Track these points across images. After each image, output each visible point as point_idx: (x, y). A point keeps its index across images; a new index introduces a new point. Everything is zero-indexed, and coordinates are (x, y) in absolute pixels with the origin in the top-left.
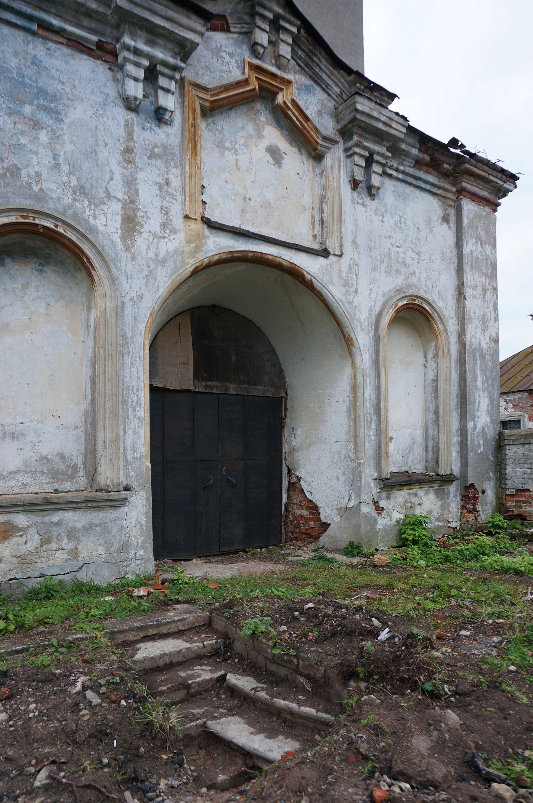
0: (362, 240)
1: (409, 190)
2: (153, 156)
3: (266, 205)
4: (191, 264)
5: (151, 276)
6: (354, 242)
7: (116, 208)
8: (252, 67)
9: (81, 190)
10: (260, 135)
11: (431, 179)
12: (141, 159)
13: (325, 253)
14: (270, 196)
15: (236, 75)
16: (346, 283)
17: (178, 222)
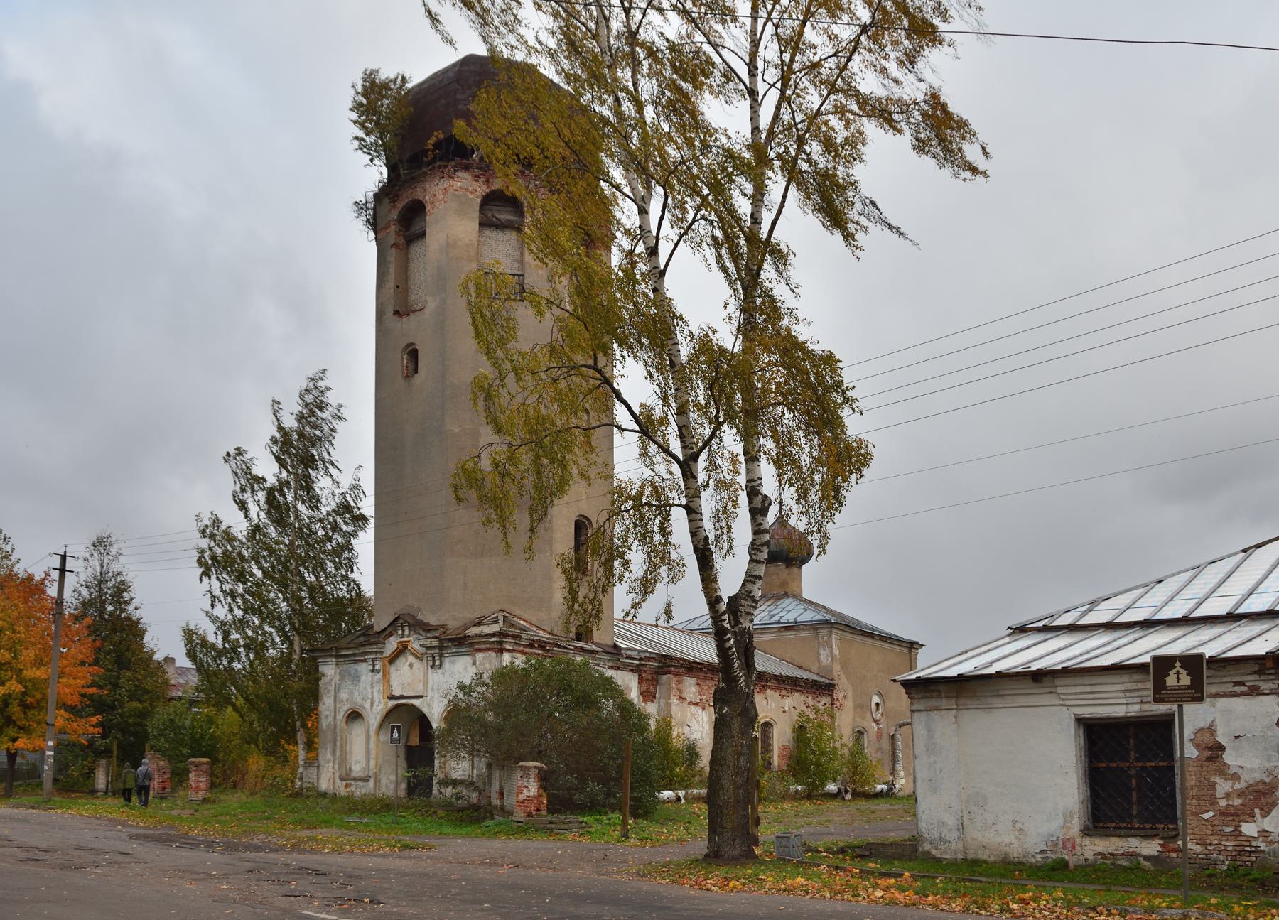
0: (435, 687)
1: (456, 658)
2: (377, 683)
3: (409, 684)
4: (385, 711)
5: (376, 718)
6: (432, 690)
7: (369, 701)
8: (399, 642)
9: (363, 699)
10: (407, 661)
11: (463, 650)
12: (374, 684)
13: (421, 697)
14: (410, 680)
15: (396, 646)
16: (429, 706)
17: (382, 700)
